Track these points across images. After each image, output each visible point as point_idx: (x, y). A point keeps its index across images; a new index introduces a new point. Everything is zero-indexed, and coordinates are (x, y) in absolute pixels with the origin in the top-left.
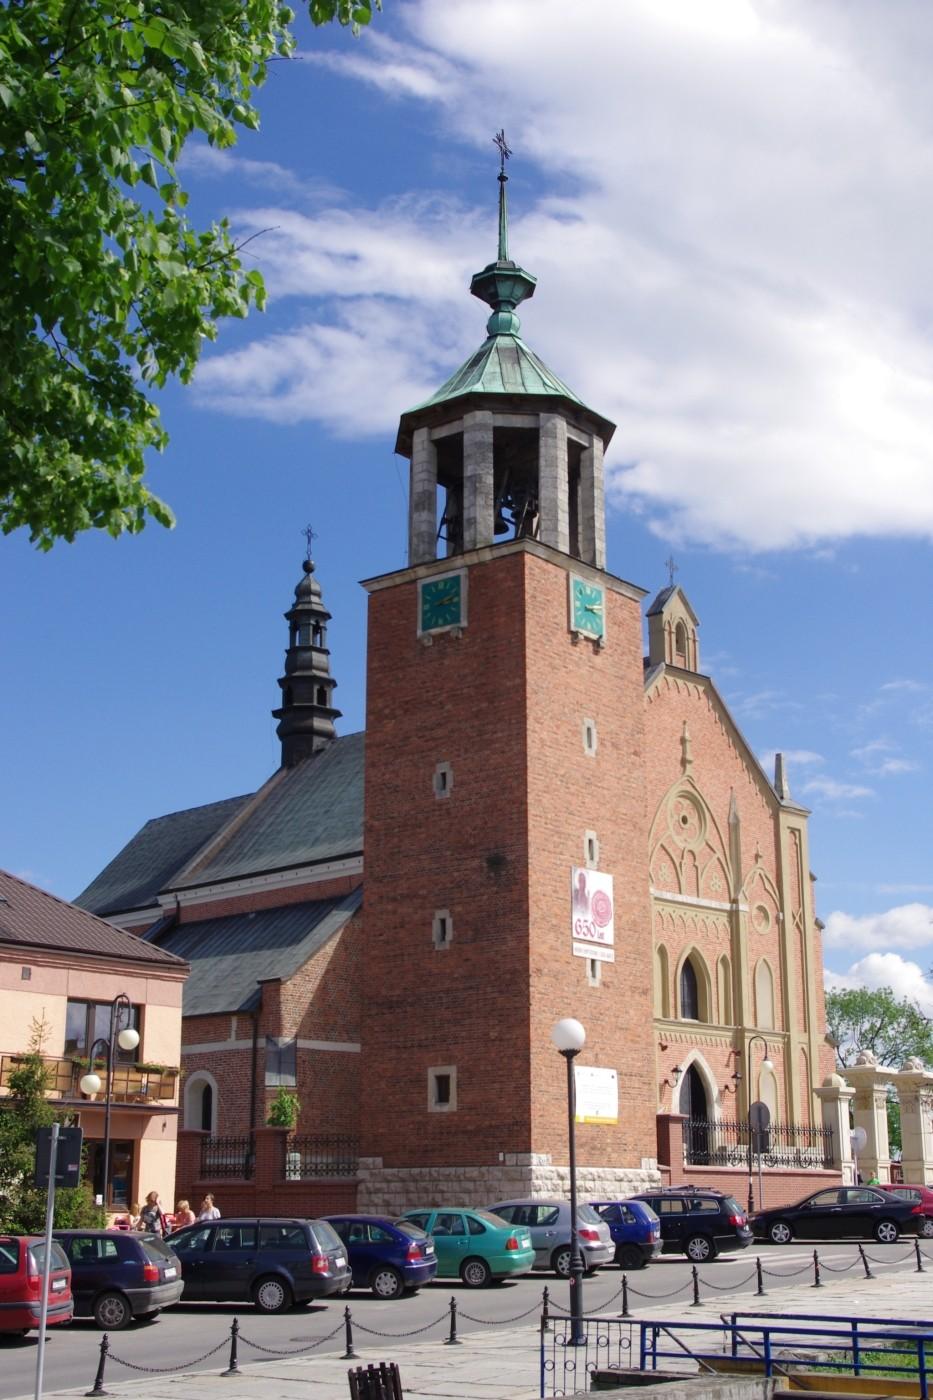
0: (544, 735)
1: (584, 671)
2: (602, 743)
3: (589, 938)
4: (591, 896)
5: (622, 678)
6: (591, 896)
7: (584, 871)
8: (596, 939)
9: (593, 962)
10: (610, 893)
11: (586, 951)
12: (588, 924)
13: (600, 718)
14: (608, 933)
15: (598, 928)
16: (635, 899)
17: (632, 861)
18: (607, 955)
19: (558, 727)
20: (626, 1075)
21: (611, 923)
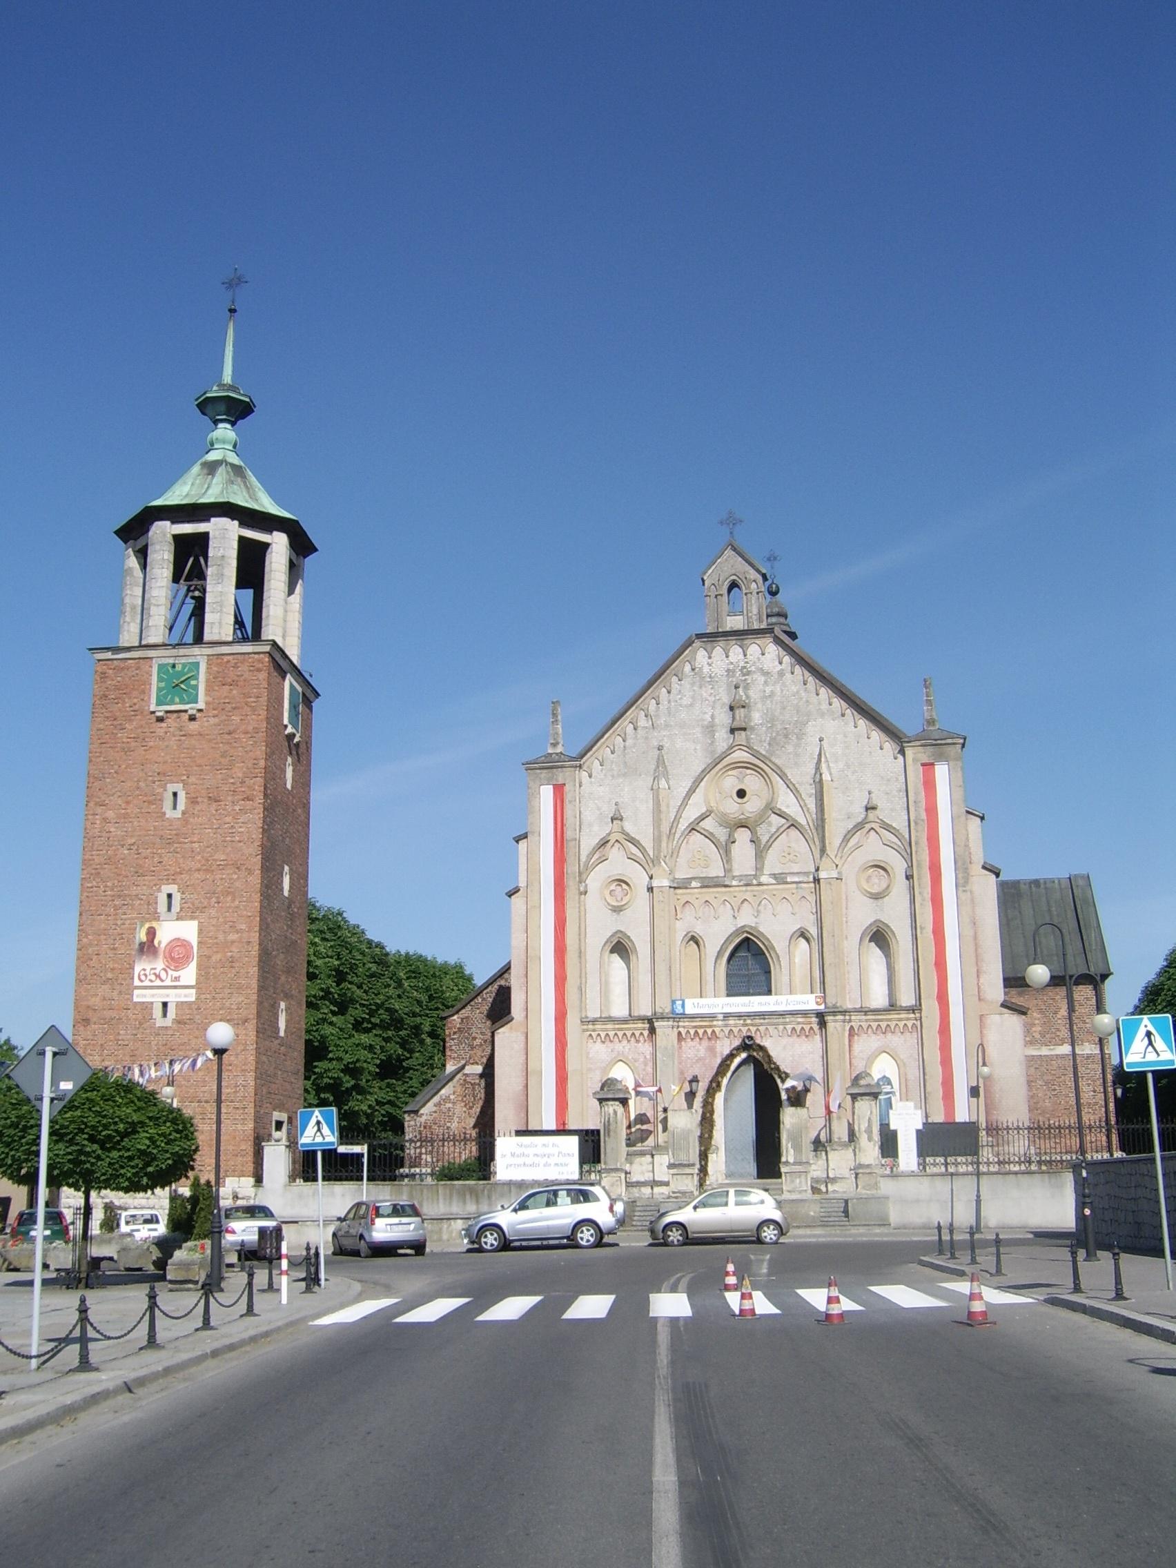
0: (110, 814)
1: (173, 743)
2: (193, 801)
3: (158, 983)
4: (163, 945)
5: (230, 733)
6: (163, 945)
7: (154, 924)
8: (168, 983)
9: (165, 1005)
10: (193, 938)
11: (153, 996)
12: (157, 972)
13: (193, 779)
14: (189, 974)
15: (170, 972)
16: (233, 937)
17: (233, 900)
18: (191, 996)
19: (128, 803)
20: (207, 1102)
21: (193, 966)
